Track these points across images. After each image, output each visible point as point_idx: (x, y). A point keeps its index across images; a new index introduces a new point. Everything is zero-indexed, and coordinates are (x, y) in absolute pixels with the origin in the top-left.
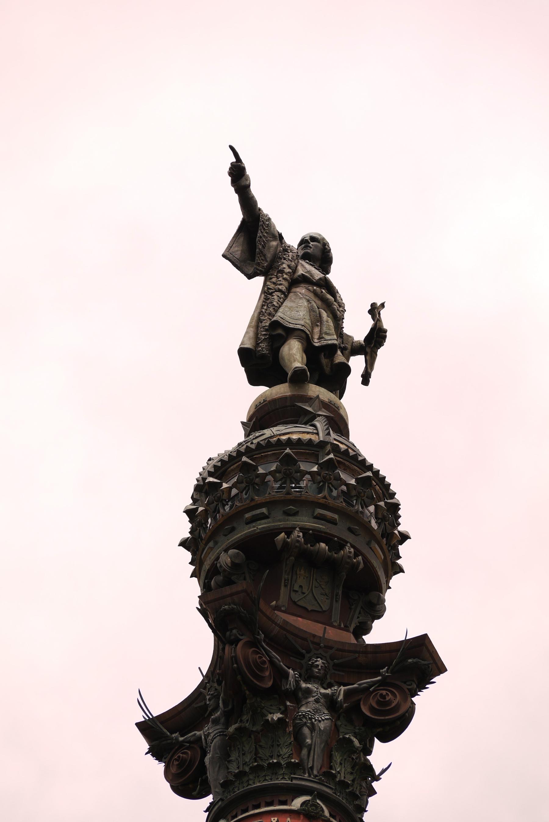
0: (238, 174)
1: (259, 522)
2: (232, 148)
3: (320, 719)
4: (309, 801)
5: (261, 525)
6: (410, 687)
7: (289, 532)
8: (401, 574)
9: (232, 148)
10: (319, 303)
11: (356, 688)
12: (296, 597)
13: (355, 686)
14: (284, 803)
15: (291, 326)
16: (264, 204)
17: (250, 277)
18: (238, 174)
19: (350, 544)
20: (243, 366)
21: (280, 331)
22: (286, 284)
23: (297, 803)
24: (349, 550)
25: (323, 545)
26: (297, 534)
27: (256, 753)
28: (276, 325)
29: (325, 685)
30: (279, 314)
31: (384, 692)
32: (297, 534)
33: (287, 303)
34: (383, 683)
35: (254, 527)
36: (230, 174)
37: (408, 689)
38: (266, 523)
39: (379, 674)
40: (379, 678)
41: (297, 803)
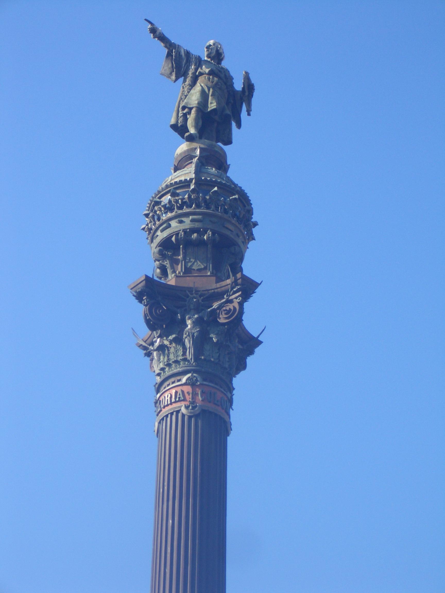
0: (153, 31)
2: (146, 20)
4: (189, 377)
5: (166, 234)
6: (239, 301)
7: (177, 234)
8: (257, 226)
9: (146, 20)
11: (214, 308)
13: (214, 307)
14: (179, 381)
15: (191, 106)
17: (175, 82)
18: (153, 31)
20: (176, 132)
25: (195, 235)
28: (184, 108)
31: (224, 308)
33: (192, 91)
36: (151, 32)
37: (238, 302)
39: (224, 298)
40: (224, 300)
41: (184, 380)
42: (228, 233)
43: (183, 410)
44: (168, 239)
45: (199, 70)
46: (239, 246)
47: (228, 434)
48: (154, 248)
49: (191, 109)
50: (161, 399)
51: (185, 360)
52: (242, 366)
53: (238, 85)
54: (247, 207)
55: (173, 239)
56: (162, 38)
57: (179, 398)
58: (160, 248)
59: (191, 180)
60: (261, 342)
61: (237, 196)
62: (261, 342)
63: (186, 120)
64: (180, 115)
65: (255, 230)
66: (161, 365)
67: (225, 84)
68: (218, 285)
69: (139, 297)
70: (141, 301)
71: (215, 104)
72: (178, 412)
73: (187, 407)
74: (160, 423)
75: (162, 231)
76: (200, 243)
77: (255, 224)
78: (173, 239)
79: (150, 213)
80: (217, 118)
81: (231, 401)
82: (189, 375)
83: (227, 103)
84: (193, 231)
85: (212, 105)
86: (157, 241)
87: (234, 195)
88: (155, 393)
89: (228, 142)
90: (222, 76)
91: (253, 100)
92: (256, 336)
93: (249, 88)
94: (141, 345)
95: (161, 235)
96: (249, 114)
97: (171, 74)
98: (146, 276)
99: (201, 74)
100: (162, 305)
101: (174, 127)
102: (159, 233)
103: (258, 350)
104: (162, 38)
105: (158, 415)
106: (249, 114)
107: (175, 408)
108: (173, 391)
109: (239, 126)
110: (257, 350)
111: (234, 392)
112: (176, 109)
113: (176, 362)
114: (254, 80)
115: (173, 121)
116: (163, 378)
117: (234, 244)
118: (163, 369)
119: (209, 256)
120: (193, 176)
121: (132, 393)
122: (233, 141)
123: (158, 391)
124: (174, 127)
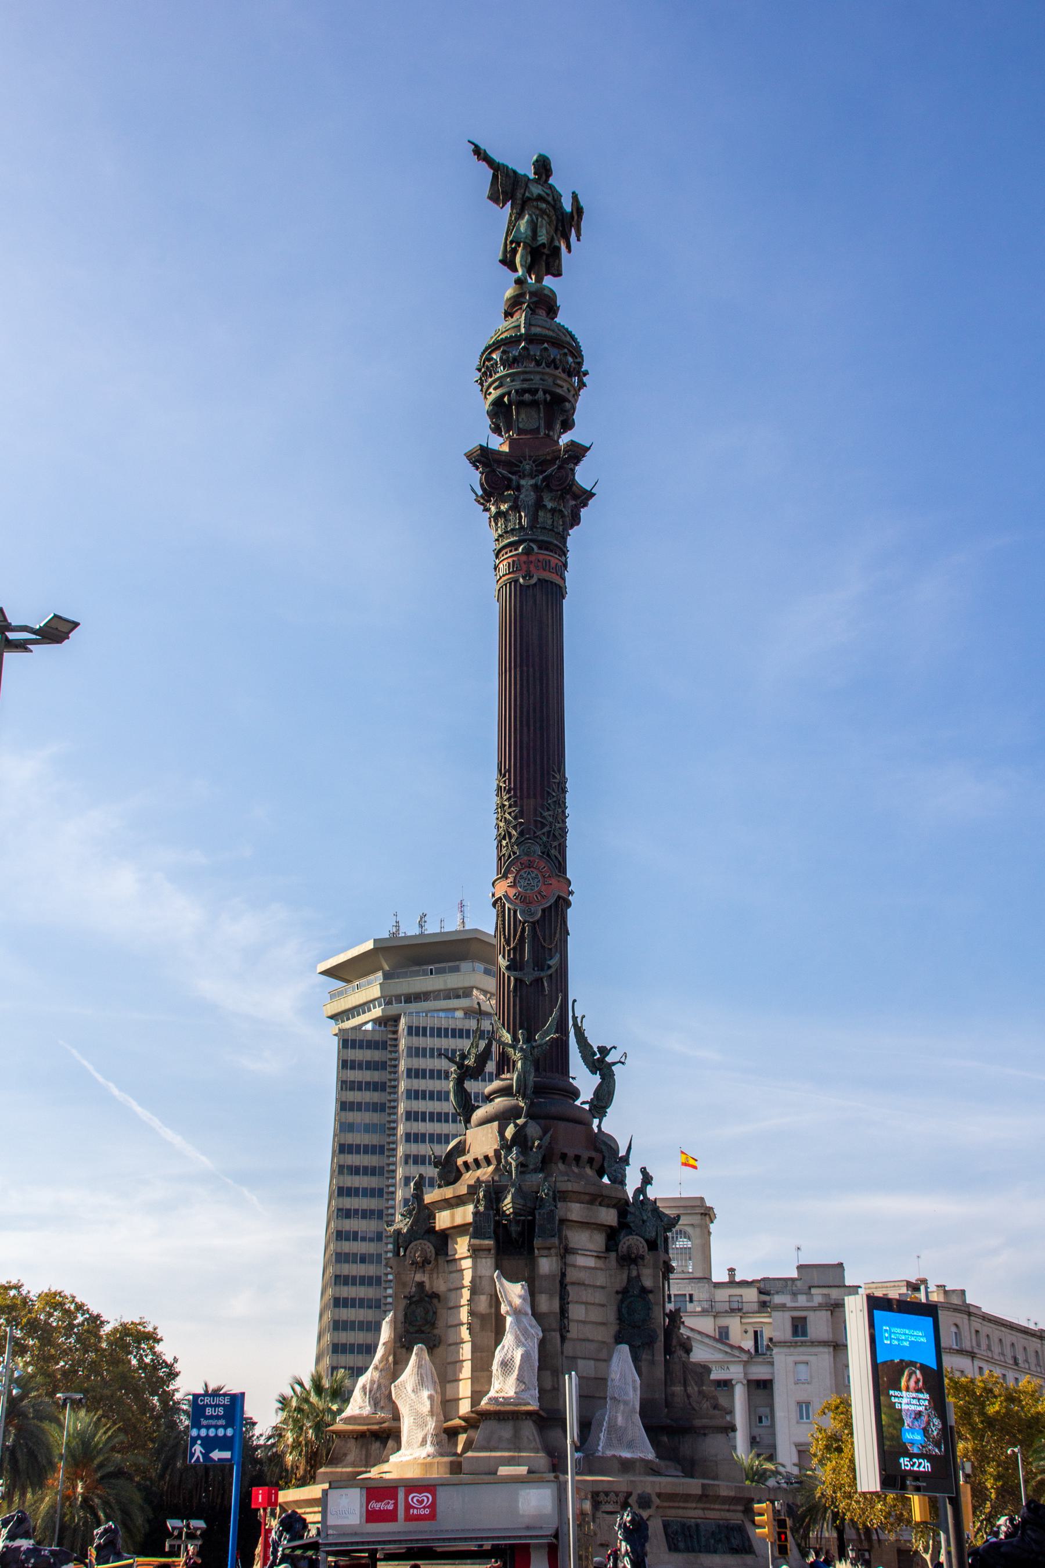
0: (478, 152)
5: (499, 392)
10: (537, 212)
12: (521, 426)
14: (516, 550)
16: (498, 159)
23: (520, 550)
24: (541, 393)
34: (560, 468)
41: (520, 550)
42: (559, 391)
43: (521, 580)
44: (502, 396)
45: (527, 194)
46: (569, 402)
47: (563, 598)
48: (487, 406)
51: (522, 527)
52: (576, 520)
53: (567, 206)
54: (579, 360)
55: (506, 399)
60: (594, 495)
62: (594, 495)
65: (585, 379)
66: (499, 531)
67: (554, 207)
70: (477, 468)
73: (524, 578)
75: (495, 389)
76: (534, 404)
77: (586, 374)
78: (506, 399)
80: (546, 251)
81: (565, 565)
83: (556, 230)
86: (491, 398)
89: (558, 274)
90: (550, 199)
91: (582, 224)
93: (579, 210)
96: (579, 240)
99: (529, 199)
100: (496, 476)
101: (503, 262)
102: (491, 390)
106: (579, 240)
108: (510, 560)
109: (570, 251)
113: (512, 530)
116: (501, 545)
117: (564, 400)
118: (500, 536)
119: (542, 415)
120: (523, 331)
121: (473, 553)
123: (497, 557)
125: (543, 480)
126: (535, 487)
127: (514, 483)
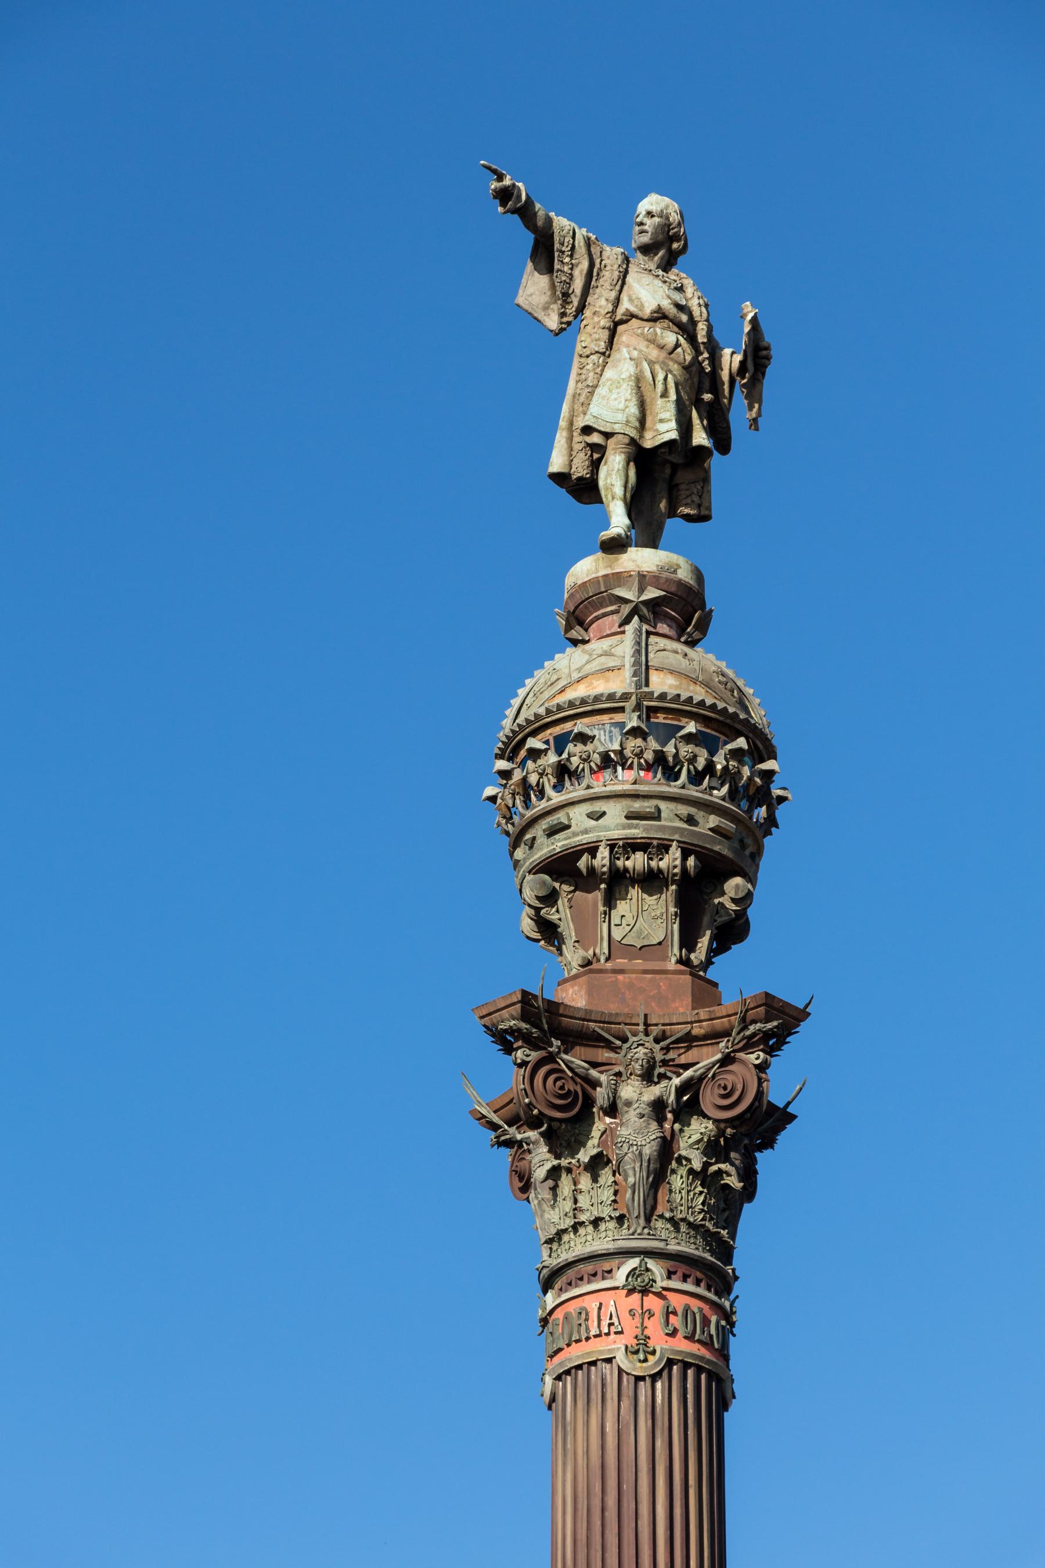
1: (557, 837)
3: (644, 1143)
19: (678, 841)
21: (596, 438)
22: (606, 333)
26: (603, 853)
27: (576, 1201)
28: (587, 430)
29: (656, 1080)
30: (594, 409)
32: (603, 853)
33: (609, 373)
34: (727, 1060)
35: (553, 844)
38: (565, 839)
41: (620, 1277)
45: (625, 305)
49: (608, 435)
50: (559, 1314)
56: (525, 213)
57: (610, 1325)
58: (546, 877)
59: (625, 697)
61: (741, 742)
63: (595, 465)
64: (577, 447)
68: (703, 1014)
69: (505, 1040)
71: (673, 424)
72: (609, 1360)
74: (559, 1378)
79: (513, 769)
82: (633, 1263)
84: (632, 846)
85: (664, 428)
87: (739, 734)
88: (538, 1288)
92: (781, 1106)
94: (484, 1117)
95: (547, 847)
97: (546, 308)
98: (524, 993)
102: (537, 832)
103: (783, 1138)
104: (525, 213)
105: (552, 1357)
107: (601, 1352)
110: (782, 1138)
111: (737, 1288)
112: (563, 423)
114: (769, 336)
115: (557, 463)
122: (714, 513)
124: (560, 479)
125: (681, 1091)
126: (658, 1107)
127: (601, 1095)
